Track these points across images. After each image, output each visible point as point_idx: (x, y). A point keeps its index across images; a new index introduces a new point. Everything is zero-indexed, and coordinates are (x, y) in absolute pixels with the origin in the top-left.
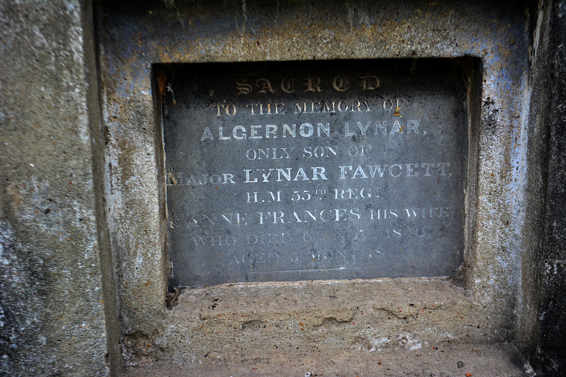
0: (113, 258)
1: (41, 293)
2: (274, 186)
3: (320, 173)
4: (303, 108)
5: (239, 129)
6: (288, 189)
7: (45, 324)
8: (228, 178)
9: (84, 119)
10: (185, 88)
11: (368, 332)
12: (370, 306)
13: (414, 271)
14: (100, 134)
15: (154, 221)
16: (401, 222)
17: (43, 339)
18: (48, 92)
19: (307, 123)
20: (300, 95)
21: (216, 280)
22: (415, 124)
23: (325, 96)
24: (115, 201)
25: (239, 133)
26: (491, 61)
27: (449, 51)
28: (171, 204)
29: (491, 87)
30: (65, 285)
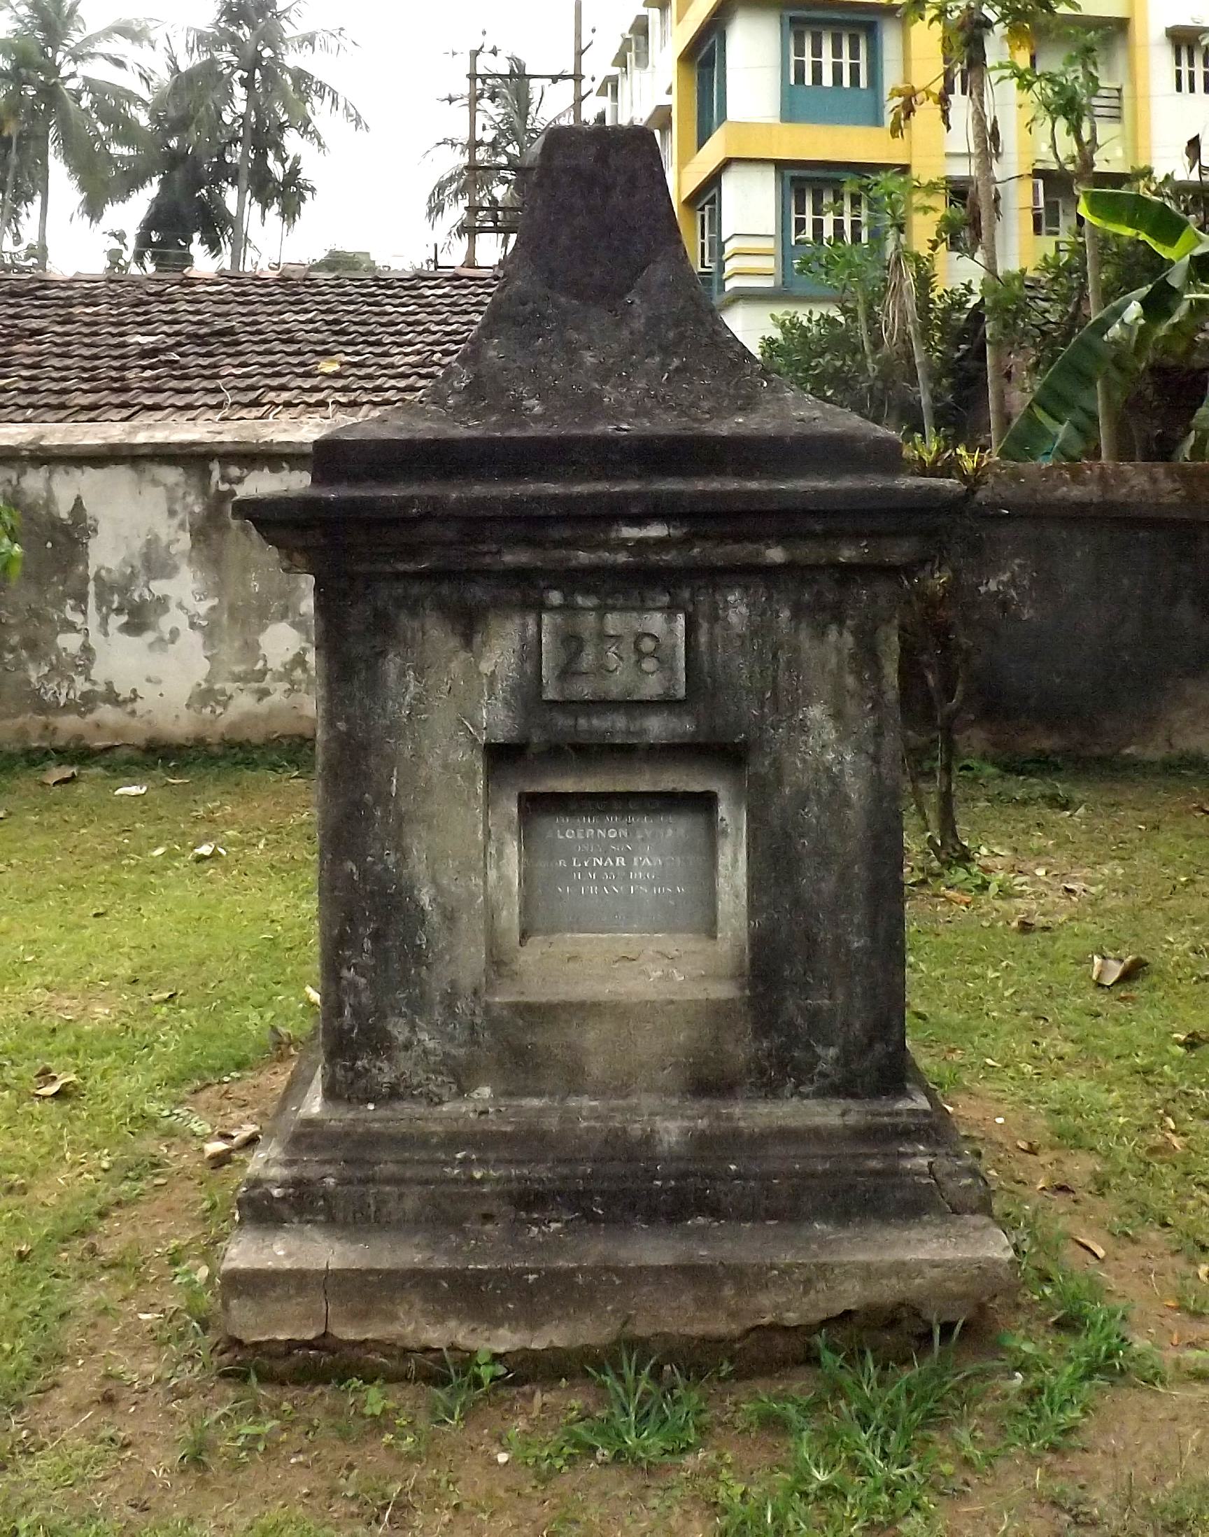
1: (449, 929)
7: (450, 947)
9: (481, 826)
17: (447, 957)
18: (462, 811)
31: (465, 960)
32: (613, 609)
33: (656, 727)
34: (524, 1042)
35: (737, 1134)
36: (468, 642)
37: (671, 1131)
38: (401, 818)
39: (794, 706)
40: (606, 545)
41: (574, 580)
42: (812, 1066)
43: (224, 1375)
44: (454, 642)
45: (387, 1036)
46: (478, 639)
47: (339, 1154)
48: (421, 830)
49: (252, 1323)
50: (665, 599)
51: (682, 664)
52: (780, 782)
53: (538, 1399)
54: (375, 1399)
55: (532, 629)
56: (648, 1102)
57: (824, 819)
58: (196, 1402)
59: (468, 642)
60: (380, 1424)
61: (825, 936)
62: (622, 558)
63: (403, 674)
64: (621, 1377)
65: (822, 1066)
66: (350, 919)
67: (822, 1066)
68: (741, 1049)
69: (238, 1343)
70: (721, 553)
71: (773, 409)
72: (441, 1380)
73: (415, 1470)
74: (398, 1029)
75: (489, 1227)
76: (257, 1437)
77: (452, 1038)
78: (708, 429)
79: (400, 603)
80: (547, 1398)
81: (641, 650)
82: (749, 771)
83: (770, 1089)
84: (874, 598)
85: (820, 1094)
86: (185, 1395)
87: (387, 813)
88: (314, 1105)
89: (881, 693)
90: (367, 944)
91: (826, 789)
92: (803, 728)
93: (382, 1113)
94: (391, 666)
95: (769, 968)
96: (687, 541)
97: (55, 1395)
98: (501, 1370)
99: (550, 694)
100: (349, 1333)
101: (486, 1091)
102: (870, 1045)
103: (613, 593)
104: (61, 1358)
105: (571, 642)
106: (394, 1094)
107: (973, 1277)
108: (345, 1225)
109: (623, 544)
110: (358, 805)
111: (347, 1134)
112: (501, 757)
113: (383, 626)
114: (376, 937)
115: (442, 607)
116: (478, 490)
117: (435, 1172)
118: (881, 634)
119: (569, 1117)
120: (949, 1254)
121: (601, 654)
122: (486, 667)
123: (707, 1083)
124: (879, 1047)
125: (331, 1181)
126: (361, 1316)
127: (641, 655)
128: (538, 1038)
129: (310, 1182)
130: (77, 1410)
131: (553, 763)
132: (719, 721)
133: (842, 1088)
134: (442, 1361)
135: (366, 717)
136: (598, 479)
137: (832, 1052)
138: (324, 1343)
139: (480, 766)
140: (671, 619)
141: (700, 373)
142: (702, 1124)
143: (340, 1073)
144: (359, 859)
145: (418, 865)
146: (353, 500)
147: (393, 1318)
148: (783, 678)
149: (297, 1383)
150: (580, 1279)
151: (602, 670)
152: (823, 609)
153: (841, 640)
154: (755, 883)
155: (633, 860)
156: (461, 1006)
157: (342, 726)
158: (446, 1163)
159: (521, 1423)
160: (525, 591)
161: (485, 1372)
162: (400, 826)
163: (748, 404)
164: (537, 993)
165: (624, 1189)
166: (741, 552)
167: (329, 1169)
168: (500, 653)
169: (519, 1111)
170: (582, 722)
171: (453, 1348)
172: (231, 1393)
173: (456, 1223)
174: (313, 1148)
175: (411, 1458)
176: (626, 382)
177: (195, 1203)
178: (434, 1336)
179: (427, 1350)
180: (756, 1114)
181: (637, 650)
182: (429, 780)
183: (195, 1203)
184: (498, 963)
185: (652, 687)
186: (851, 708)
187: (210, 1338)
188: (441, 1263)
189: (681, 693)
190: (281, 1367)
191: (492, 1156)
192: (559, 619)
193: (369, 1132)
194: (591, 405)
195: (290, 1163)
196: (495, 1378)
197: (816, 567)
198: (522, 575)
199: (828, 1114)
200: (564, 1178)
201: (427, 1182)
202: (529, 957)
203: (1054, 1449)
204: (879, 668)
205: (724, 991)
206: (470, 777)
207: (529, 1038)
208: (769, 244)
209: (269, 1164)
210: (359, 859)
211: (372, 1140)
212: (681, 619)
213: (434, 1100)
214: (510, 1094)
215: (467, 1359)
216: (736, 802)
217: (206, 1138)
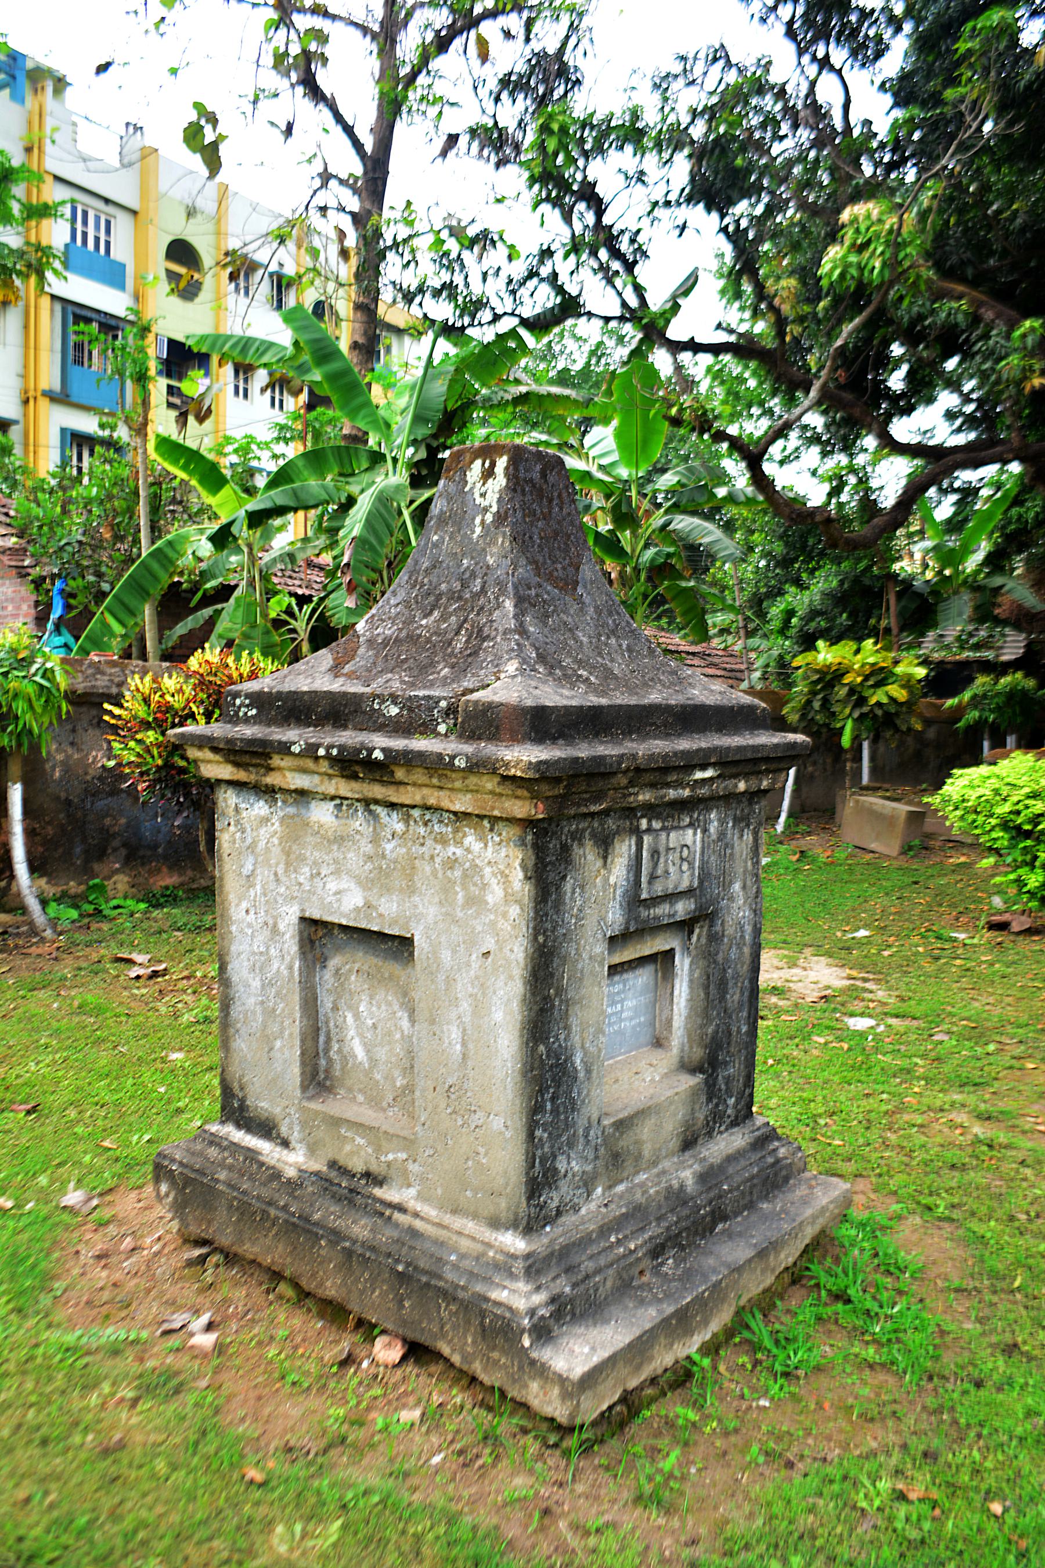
40: (679, 784)
41: (651, 810)
44: (599, 863)
48: (577, 1007)
66: (540, 1091)
94: (568, 886)
99: (644, 896)
110: (546, 999)
111: (552, 1254)
113: (565, 854)
115: (594, 836)
122: (612, 880)
125: (568, 1289)
153: (748, 837)
174: (538, 1272)
185: (684, 885)
195: (538, 1288)
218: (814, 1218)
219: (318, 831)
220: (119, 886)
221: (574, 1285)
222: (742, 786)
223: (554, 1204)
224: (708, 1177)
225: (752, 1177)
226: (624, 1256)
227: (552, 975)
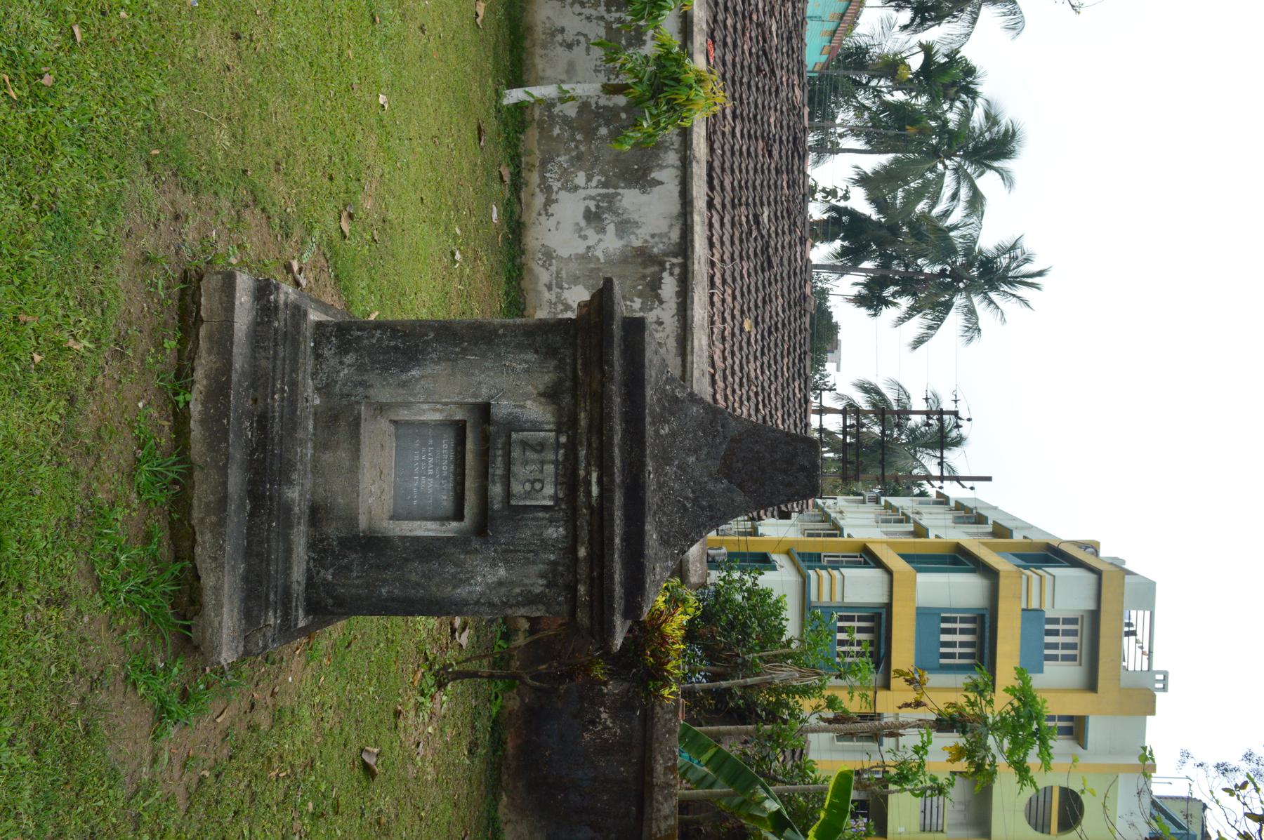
0: (407, 405)
2: (427, 457)
3: (431, 472)
4: (452, 467)
5: (446, 448)
6: (426, 461)
8: (431, 442)
10: (459, 429)
11: (377, 485)
12: (385, 486)
13: (395, 504)
14: (446, 404)
15: (418, 418)
16: (412, 499)
19: (447, 468)
20: (456, 466)
21: (397, 437)
22: (445, 503)
23: (455, 474)
24: (425, 407)
25: (445, 446)
26: (463, 524)
27: (466, 511)
28: (424, 424)
29: (454, 524)
30: (401, 391)
31: (383, 393)
32: (557, 469)
33: (496, 490)
34: (341, 421)
35: (291, 527)
36: (540, 395)
37: (293, 494)
38: (455, 360)
39: (506, 561)
41: (572, 448)
42: (323, 566)
43: (185, 272)
44: (541, 388)
45: (347, 353)
46: (543, 400)
47: (289, 328)
49: (210, 285)
50: (561, 495)
51: (528, 503)
52: (467, 553)
53: (166, 423)
54: (171, 344)
55: (547, 427)
56: (308, 484)
57: (447, 576)
58: (173, 259)
59: (540, 395)
60: (159, 346)
61: (388, 575)
62: (582, 473)
63: (526, 362)
64: (174, 464)
65: (323, 572)
66: (405, 335)
67: (323, 572)
68: (332, 530)
69: (201, 278)
70: (583, 522)
71: (661, 554)
72: (178, 377)
73: (137, 362)
74: (350, 359)
75: (250, 402)
76: (156, 288)
77: (344, 385)
78: (649, 519)
79: (561, 360)
80: (167, 428)
81: (535, 481)
82: (473, 538)
83: (311, 546)
84: (558, 603)
85: (309, 570)
86: (177, 253)
87: (458, 354)
88: (314, 316)
89: (511, 607)
90: (392, 344)
91: (462, 576)
92: (494, 565)
93: (309, 350)
94: (531, 356)
95: (374, 545)
96: (590, 507)
97: (180, 192)
98: (181, 406)
99: (514, 435)
100: (203, 332)
101: (317, 402)
102: (332, 597)
103: (565, 468)
104: (196, 194)
105: (540, 447)
106: (318, 357)
107: (212, 642)
108: (255, 331)
109: (588, 473)
110: (462, 339)
112: (484, 411)
113: (550, 352)
114: (396, 348)
116: (617, 400)
117: (279, 375)
118: (540, 607)
119: (302, 443)
120: (225, 631)
121: (533, 462)
122: (529, 403)
123: (316, 513)
124: (330, 601)
125: (276, 324)
126: (210, 338)
127: (533, 483)
128: (343, 430)
129: (276, 314)
130: (173, 203)
131: (480, 436)
132: (499, 522)
133: (311, 583)
134: (187, 377)
135: (505, 344)
136: (622, 461)
137: (330, 577)
138: (199, 320)
139: (480, 400)
140: (551, 497)
141: (682, 518)
142: (297, 510)
143: (329, 329)
144: (436, 339)
145: (431, 369)
146: (612, 337)
147: (209, 353)
148: (521, 555)
149: (180, 308)
150: (223, 445)
151: (526, 463)
152: (554, 577)
153: (538, 586)
154: (417, 539)
155: (431, 478)
156: (360, 389)
157: (501, 332)
158: (283, 381)
159: (156, 415)
160: (566, 423)
161: (180, 398)
162: (449, 360)
163: (664, 541)
164: (366, 429)
165: (266, 469)
166: (584, 534)
167: (282, 324)
168: (536, 411)
169: (307, 418)
170: (500, 452)
171: (193, 382)
172: (176, 275)
173: (254, 385)
174: (293, 315)
175: (143, 361)
176: (678, 478)
177: (267, 257)
178: (199, 374)
179: (193, 370)
180: (300, 538)
181: (535, 481)
182: (473, 374)
183: (267, 257)
184: (381, 409)
185: (516, 488)
186: (503, 590)
187: (203, 265)
188: (235, 378)
189: (513, 503)
190: (188, 299)
191: (285, 403)
192: (552, 441)
193: (299, 344)
194: (664, 459)
195: (286, 305)
196: (178, 402)
197: (575, 574)
198: (574, 421)
199: (298, 574)
200: (273, 439)
201: (274, 371)
202: (384, 424)
203: (127, 677)
204: (524, 605)
205: (363, 523)
206: (474, 395)
207: (343, 423)
208: (838, 598)
209: (287, 292)
210: (436, 339)
211: (295, 344)
212: (549, 503)
213: (314, 375)
214: (315, 414)
215: (188, 388)
216: (460, 531)
217: (300, 261)
218: (218, 589)
219: (575, 280)
220: (511, 702)
221: (276, 330)
222: (582, 552)
223: (327, 353)
224: (287, 509)
225: (268, 564)
226: (274, 385)
227: (476, 344)
